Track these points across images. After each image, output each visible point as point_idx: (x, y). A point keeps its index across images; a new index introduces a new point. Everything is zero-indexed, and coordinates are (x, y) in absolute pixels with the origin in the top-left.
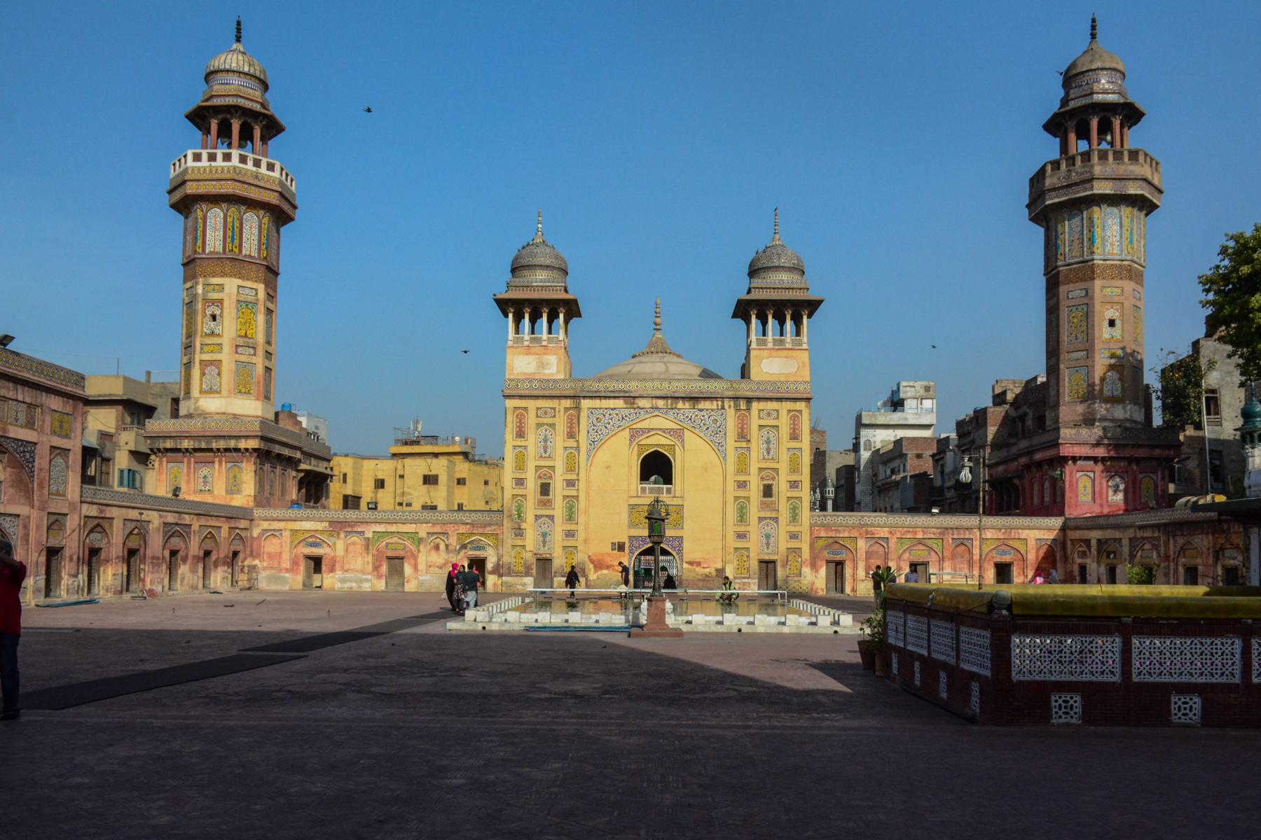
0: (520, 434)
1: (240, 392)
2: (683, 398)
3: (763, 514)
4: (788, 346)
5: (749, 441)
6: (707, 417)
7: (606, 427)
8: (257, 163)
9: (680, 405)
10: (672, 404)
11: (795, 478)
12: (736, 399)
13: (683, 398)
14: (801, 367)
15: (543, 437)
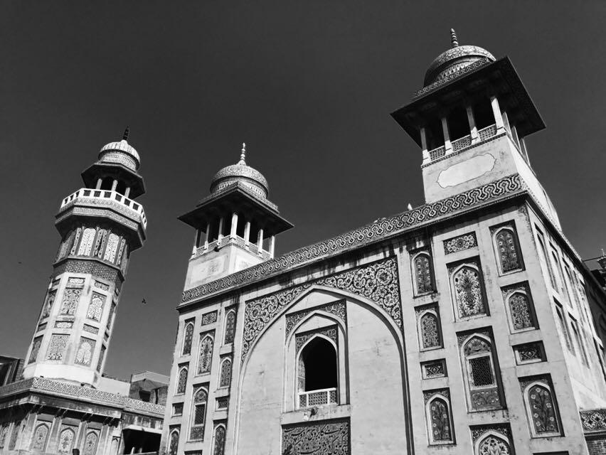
0: (187, 350)
1: (51, 359)
2: (342, 258)
3: (478, 420)
4: (474, 142)
5: (436, 292)
6: (372, 273)
7: (261, 320)
8: (97, 194)
9: (339, 269)
10: (329, 271)
11: (529, 336)
12: (407, 239)
13: (342, 258)
14: (499, 160)
15: (204, 348)
